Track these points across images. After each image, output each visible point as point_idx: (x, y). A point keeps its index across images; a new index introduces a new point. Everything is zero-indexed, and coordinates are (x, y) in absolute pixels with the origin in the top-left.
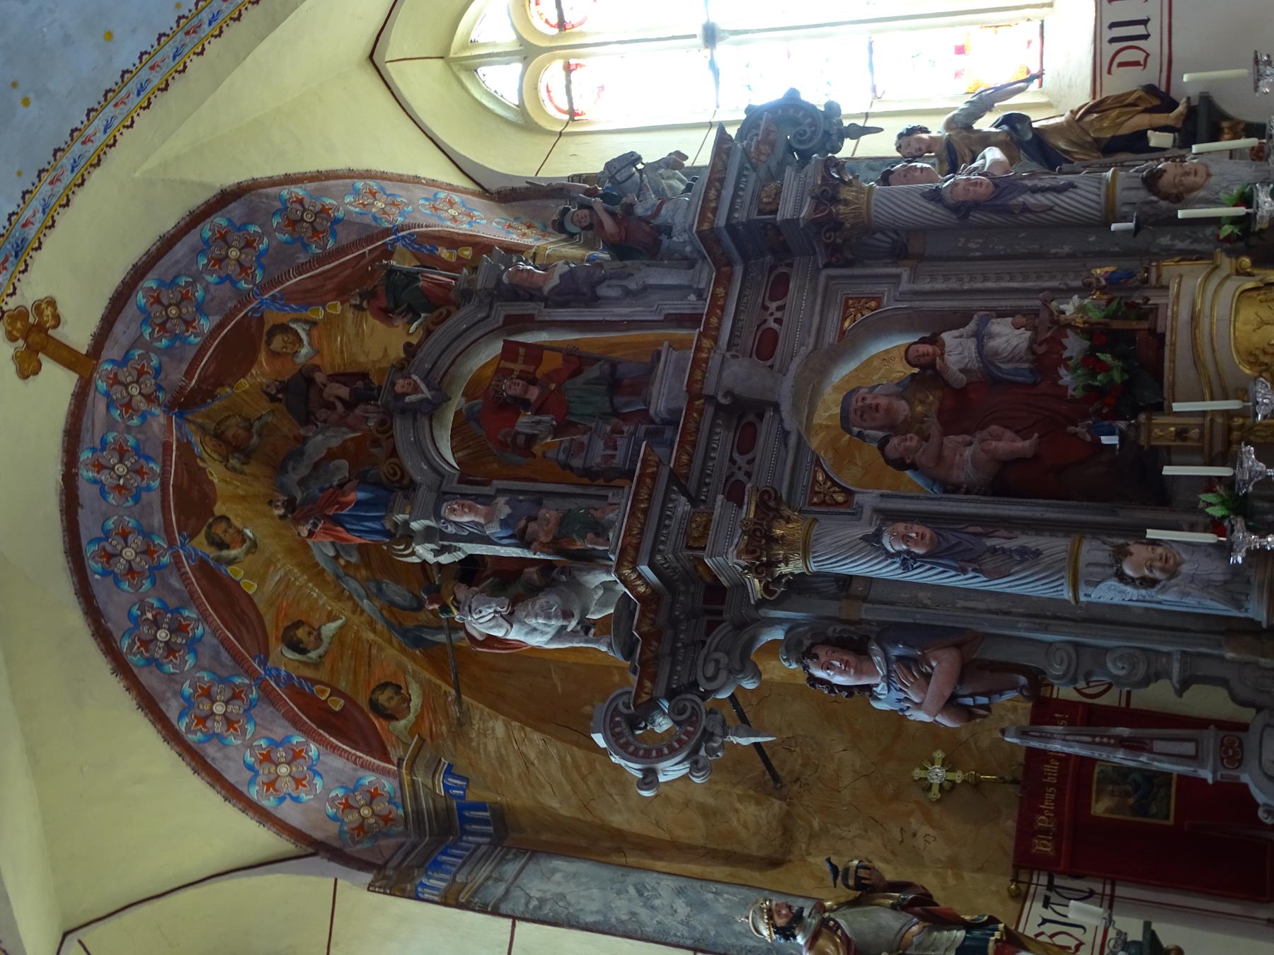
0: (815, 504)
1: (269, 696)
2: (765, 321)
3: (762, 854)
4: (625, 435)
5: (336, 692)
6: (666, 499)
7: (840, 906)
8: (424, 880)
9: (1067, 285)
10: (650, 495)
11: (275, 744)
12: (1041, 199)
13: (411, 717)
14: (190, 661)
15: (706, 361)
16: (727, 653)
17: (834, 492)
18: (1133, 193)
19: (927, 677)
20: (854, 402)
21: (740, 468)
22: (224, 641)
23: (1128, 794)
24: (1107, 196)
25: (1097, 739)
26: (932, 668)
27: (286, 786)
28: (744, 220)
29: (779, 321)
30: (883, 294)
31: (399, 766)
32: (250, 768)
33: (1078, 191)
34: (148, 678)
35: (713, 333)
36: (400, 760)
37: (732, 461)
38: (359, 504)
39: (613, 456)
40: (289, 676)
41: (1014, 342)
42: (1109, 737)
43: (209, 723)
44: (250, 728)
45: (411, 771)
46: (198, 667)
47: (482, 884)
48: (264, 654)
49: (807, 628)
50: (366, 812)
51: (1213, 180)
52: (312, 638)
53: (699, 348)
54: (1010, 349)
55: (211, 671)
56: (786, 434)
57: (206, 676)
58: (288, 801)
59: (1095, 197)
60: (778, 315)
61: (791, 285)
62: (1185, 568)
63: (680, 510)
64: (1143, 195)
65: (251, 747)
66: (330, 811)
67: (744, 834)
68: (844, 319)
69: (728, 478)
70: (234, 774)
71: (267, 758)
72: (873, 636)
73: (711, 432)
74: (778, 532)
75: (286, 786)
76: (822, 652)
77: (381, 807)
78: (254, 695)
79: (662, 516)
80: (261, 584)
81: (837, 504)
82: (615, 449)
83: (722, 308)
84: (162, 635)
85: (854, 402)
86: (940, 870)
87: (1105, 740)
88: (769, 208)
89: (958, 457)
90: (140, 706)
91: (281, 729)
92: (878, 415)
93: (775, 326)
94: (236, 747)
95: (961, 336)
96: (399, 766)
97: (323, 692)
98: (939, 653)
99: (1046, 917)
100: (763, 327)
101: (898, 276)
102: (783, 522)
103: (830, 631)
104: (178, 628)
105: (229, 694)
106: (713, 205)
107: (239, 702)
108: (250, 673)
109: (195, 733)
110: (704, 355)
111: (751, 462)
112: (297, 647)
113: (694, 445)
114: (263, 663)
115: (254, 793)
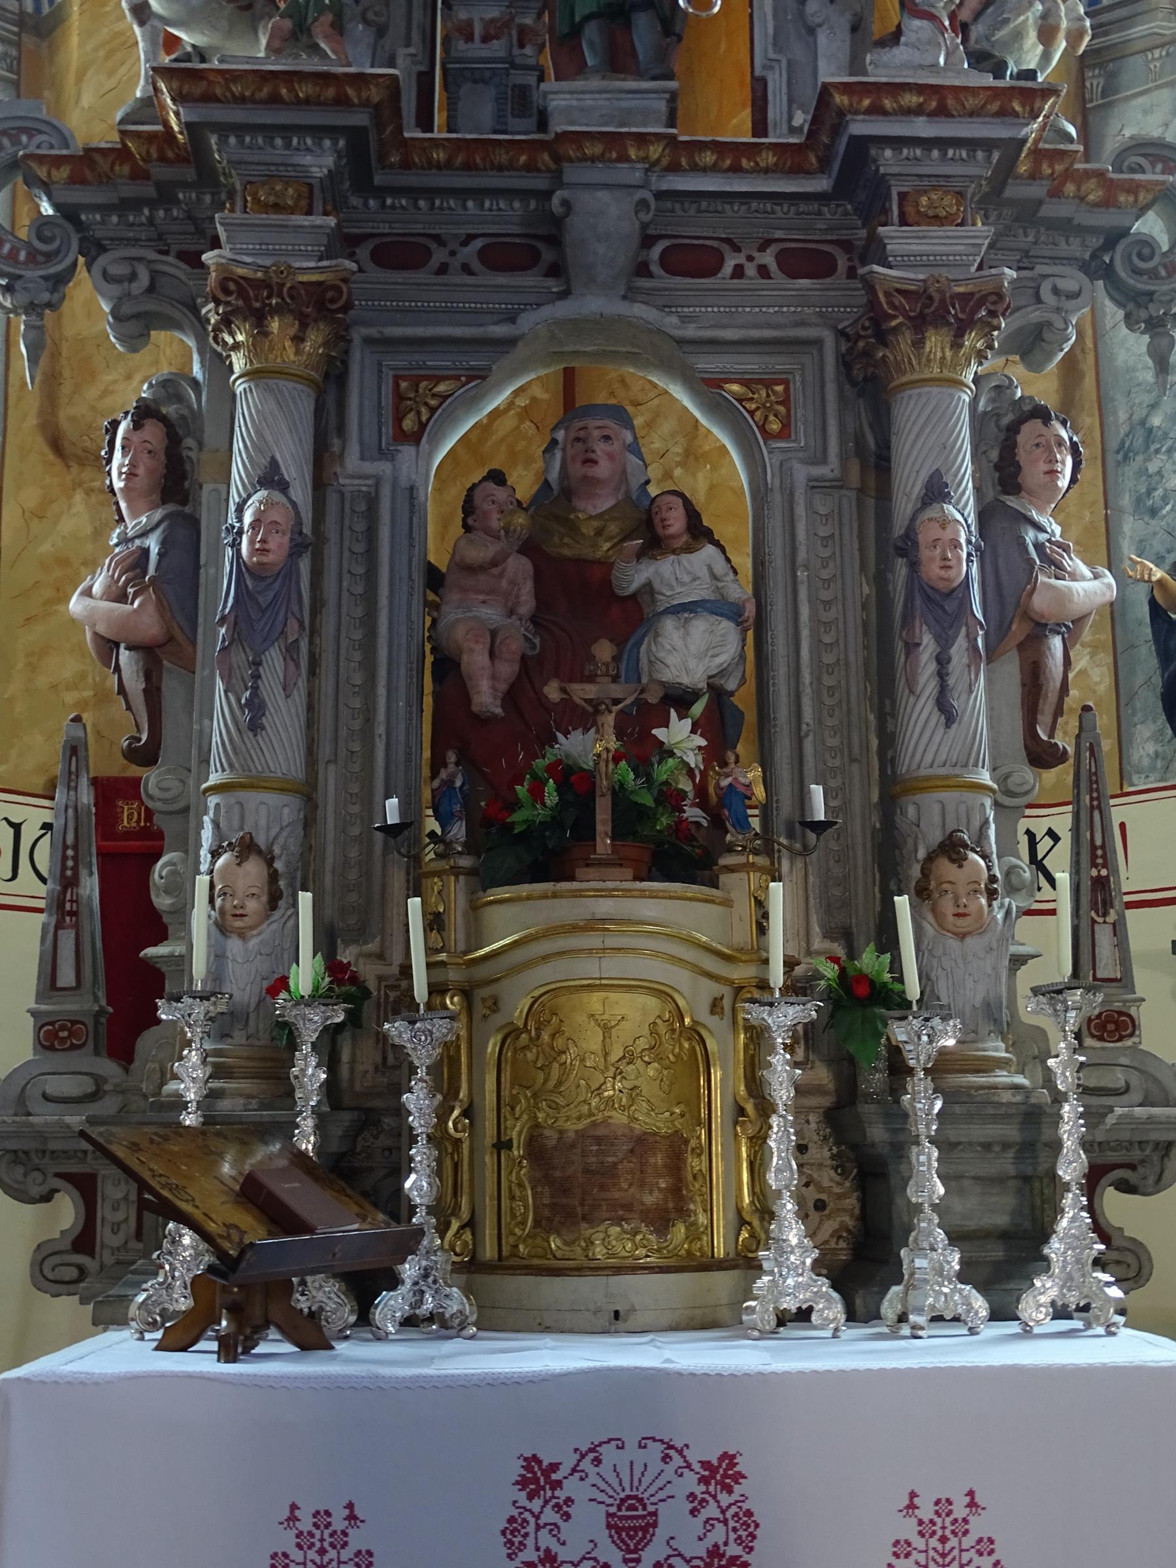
0: (396, 385)
2: (737, 249)
3: (65, 425)
4: (516, 51)
6: (319, 131)
9: (807, 735)
10: (307, 101)
12: (927, 668)
15: (624, 158)
16: (151, 289)
17: (419, 413)
18: (937, 819)
19: (122, 598)
20: (600, 423)
21: (453, 253)
24: (928, 778)
25: (70, 852)
26: (132, 603)
28: (882, 170)
29: (738, 272)
30: (794, 441)
33: (941, 730)
35: (684, 162)
37: (471, 237)
39: (470, 38)
41: (671, 660)
42: (75, 869)
49: (195, 406)
51: (953, 943)
53: (642, 139)
54: (661, 655)
56: (512, 319)
59: (929, 758)
60: (751, 270)
61: (804, 282)
62: (234, 945)
63: (308, 160)
64: (935, 836)
67: (92, 393)
68: (744, 383)
69: (437, 238)
72: (187, 509)
73: (509, 193)
74: (275, 325)
76: (153, 432)
79: (286, 130)
81: (398, 420)
82: (485, 39)
83: (736, 169)
85: (600, 423)
86: (90, 680)
87: (70, 863)
88: (910, 210)
89: (481, 597)
92: (578, 465)
93: (728, 268)
95: (714, 577)
98: (151, 608)
99: (23, 827)
100: (725, 248)
101: (824, 461)
102: (292, 331)
103: (189, 442)
106: (888, 103)
110: (633, 153)
111: (467, 269)
113: (469, 167)
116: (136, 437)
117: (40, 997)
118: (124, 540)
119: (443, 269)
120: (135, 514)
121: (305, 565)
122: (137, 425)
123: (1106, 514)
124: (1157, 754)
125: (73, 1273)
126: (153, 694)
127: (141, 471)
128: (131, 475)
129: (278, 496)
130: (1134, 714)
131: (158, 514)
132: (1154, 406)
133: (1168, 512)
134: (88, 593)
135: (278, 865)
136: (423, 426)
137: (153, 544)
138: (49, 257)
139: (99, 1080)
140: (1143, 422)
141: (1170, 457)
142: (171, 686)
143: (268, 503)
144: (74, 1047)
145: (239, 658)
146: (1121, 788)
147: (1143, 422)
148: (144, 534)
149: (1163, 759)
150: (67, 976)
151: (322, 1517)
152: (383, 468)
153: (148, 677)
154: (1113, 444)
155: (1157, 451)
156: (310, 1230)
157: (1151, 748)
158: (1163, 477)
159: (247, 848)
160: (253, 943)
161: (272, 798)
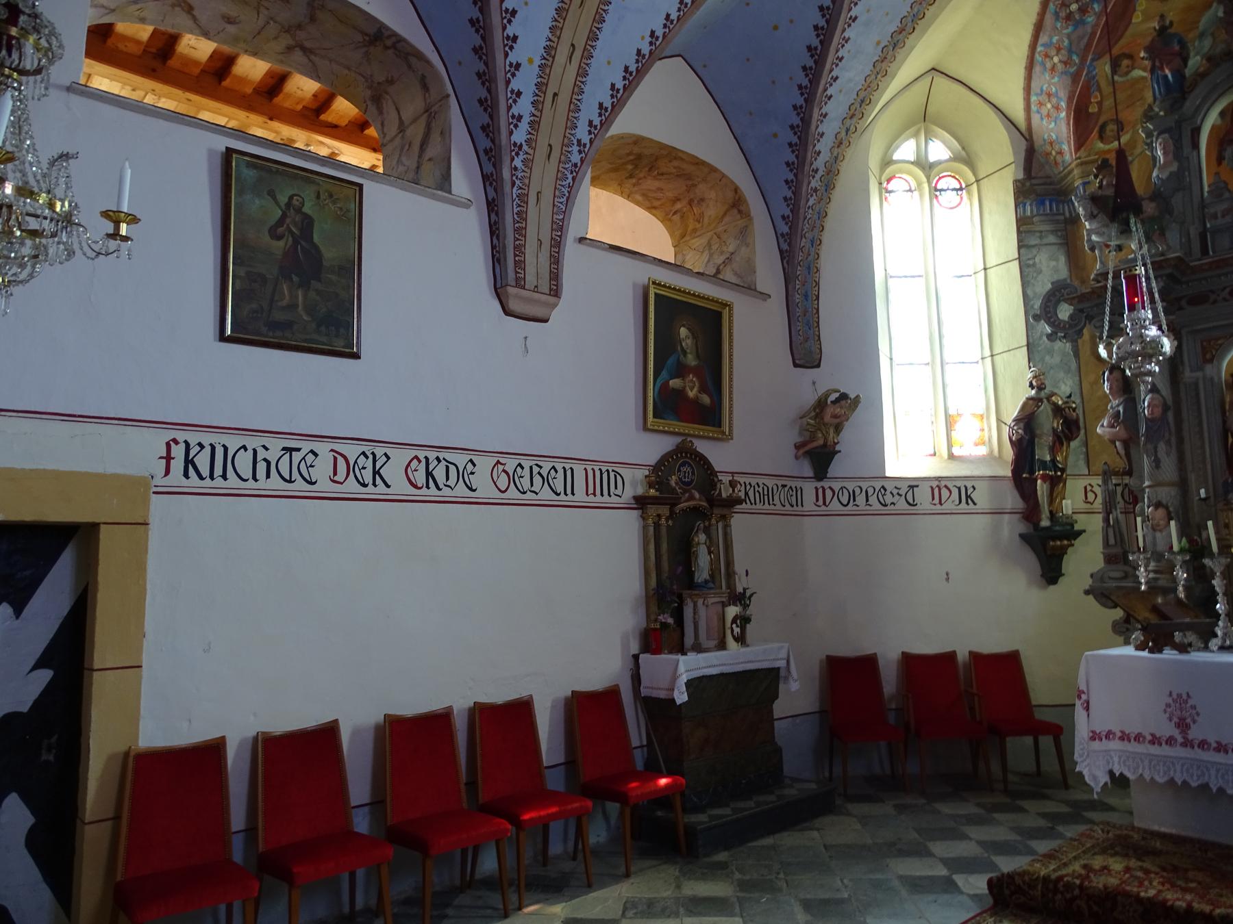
1: (1075, 78)
5: (1100, 104)
7: (1055, 405)
8: (1028, 204)
11: (1056, 95)
13: (1107, 147)
14: (1070, 29)
19: (1112, 426)
21: (1218, 295)
22: (1093, 34)
27: (1044, 111)
31: (1076, 159)
32: (1042, 90)
34: (1049, 18)
36: (1079, 158)
38: (1166, 76)
40: (1094, 77)
42: (1111, 509)
43: (1047, 60)
44: (1056, 79)
45: (1077, 166)
46: (1069, 36)
47: (1035, 231)
48: (1098, 57)
50: (1054, 153)
52: (1126, 70)
55: (1071, 44)
57: (1066, 43)
58: (1039, 116)
62: (1158, 534)
65: (1049, 85)
66: (1046, 137)
69: (1213, 292)
70: (1035, 85)
71: (1049, 95)
75: (1044, 111)
77: (1059, 159)
78: (1072, 70)
80: (1143, 21)
82: (1223, 216)
84: (1074, 7)
90: (1035, 24)
91: (1063, 95)
94: (1045, 79)
96: (1076, 159)
97: (1096, 97)
104: (1083, 10)
105: (1065, 59)
107: (1064, 66)
108: (1083, 60)
109: (1040, 56)
111: (1225, 300)
112: (1115, 66)
114: (1093, 60)
115: (1034, 99)
116: (1111, 377)
117: (1104, 548)
118: (1112, 407)
119: (1215, 302)
120: (1115, 399)
121: (1170, 415)
122: (1111, 373)
125: (1125, 630)
126: (1128, 455)
127: (1114, 386)
128: (1111, 389)
129: (1156, 396)
131: (1122, 399)
134: (1102, 426)
135: (1171, 509)
136: (1214, 356)
137: (1121, 409)
138: (1076, 325)
139: (1126, 573)
142: (1133, 452)
143: (1152, 399)
144: (1117, 563)
145: (1150, 446)
148: (1118, 406)
150: (1112, 541)
151: (1180, 696)
152: (1199, 374)
153: (1125, 449)
156: (1171, 619)
159: (1158, 505)
160: (1164, 533)
161: (1166, 489)
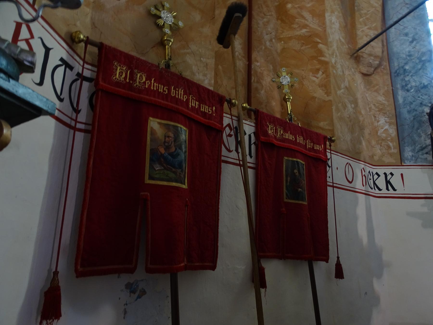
23: (167, 148)
123: (392, 89)
124: (413, 156)
130: (405, 143)
132: (406, 64)
133: (413, 92)
140: (403, 67)
141: (412, 77)
146: (401, 163)
147: (403, 67)
149: (415, 157)
154: (393, 71)
155: (408, 75)
157: (411, 154)
158: (410, 82)
